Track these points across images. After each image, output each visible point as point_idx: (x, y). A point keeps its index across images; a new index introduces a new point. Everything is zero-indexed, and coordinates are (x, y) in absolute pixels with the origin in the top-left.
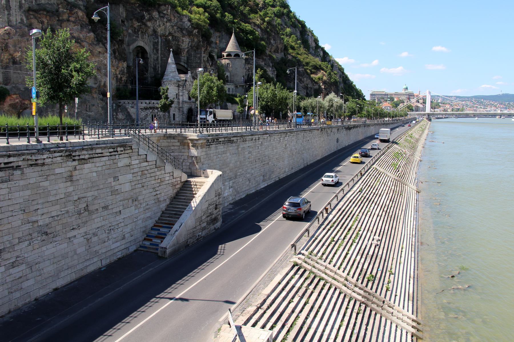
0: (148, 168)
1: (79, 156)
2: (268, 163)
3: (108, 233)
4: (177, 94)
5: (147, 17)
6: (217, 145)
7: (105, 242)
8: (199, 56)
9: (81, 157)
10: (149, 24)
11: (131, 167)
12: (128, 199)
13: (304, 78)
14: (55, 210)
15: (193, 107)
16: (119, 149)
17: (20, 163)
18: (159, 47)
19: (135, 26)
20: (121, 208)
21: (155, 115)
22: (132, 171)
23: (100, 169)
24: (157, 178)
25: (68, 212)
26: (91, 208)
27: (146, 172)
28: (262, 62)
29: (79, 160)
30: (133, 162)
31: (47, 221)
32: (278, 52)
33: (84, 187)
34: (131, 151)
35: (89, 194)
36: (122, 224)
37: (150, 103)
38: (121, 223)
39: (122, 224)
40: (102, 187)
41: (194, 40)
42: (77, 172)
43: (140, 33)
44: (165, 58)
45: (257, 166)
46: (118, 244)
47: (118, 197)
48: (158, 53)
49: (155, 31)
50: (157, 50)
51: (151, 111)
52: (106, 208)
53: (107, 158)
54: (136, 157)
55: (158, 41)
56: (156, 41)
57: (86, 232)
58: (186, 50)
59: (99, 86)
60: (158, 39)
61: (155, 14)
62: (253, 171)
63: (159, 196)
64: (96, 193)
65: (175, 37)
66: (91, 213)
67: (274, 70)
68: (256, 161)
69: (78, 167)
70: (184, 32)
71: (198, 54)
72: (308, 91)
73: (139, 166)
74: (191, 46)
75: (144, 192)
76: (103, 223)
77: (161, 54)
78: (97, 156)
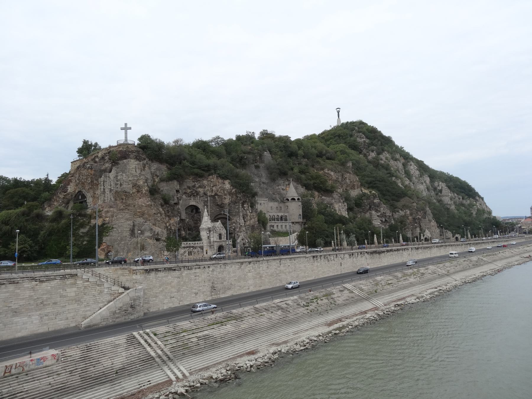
0: (89, 285)
1: (40, 279)
2: (222, 283)
3: (56, 316)
4: (208, 237)
6: (157, 272)
7: (53, 320)
8: (237, 207)
9: (41, 280)
11: (76, 285)
12: (73, 300)
13: (380, 208)
14: (22, 303)
15: (224, 245)
16: (66, 276)
17: (5, 283)
19: (188, 192)
20: (67, 304)
21: (191, 252)
22: (77, 287)
23: (53, 285)
24: (97, 290)
25: (29, 304)
26: (45, 303)
27: (88, 287)
29: (39, 281)
30: (78, 282)
31: (17, 307)
32: (355, 189)
33: (41, 293)
34: (77, 277)
35: (44, 296)
36: (67, 312)
37: (187, 244)
38: (66, 311)
39: (67, 312)
40: (54, 293)
41: (233, 197)
42: (38, 287)
43: (192, 196)
44: (213, 211)
45: (205, 284)
46: (63, 321)
47: (65, 298)
49: (205, 194)
51: (188, 249)
52: (55, 303)
53: (59, 280)
54: (80, 280)
55: (208, 200)
56: (206, 200)
57: (40, 314)
59: (154, 235)
60: (208, 198)
63: (98, 300)
64: (49, 296)
66: (44, 305)
67: (345, 205)
68: (204, 282)
69: (38, 284)
71: (237, 206)
72: (387, 219)
73: (82, 284)
75: (85, 297)
76: (53, 310)
78: (51, 279)
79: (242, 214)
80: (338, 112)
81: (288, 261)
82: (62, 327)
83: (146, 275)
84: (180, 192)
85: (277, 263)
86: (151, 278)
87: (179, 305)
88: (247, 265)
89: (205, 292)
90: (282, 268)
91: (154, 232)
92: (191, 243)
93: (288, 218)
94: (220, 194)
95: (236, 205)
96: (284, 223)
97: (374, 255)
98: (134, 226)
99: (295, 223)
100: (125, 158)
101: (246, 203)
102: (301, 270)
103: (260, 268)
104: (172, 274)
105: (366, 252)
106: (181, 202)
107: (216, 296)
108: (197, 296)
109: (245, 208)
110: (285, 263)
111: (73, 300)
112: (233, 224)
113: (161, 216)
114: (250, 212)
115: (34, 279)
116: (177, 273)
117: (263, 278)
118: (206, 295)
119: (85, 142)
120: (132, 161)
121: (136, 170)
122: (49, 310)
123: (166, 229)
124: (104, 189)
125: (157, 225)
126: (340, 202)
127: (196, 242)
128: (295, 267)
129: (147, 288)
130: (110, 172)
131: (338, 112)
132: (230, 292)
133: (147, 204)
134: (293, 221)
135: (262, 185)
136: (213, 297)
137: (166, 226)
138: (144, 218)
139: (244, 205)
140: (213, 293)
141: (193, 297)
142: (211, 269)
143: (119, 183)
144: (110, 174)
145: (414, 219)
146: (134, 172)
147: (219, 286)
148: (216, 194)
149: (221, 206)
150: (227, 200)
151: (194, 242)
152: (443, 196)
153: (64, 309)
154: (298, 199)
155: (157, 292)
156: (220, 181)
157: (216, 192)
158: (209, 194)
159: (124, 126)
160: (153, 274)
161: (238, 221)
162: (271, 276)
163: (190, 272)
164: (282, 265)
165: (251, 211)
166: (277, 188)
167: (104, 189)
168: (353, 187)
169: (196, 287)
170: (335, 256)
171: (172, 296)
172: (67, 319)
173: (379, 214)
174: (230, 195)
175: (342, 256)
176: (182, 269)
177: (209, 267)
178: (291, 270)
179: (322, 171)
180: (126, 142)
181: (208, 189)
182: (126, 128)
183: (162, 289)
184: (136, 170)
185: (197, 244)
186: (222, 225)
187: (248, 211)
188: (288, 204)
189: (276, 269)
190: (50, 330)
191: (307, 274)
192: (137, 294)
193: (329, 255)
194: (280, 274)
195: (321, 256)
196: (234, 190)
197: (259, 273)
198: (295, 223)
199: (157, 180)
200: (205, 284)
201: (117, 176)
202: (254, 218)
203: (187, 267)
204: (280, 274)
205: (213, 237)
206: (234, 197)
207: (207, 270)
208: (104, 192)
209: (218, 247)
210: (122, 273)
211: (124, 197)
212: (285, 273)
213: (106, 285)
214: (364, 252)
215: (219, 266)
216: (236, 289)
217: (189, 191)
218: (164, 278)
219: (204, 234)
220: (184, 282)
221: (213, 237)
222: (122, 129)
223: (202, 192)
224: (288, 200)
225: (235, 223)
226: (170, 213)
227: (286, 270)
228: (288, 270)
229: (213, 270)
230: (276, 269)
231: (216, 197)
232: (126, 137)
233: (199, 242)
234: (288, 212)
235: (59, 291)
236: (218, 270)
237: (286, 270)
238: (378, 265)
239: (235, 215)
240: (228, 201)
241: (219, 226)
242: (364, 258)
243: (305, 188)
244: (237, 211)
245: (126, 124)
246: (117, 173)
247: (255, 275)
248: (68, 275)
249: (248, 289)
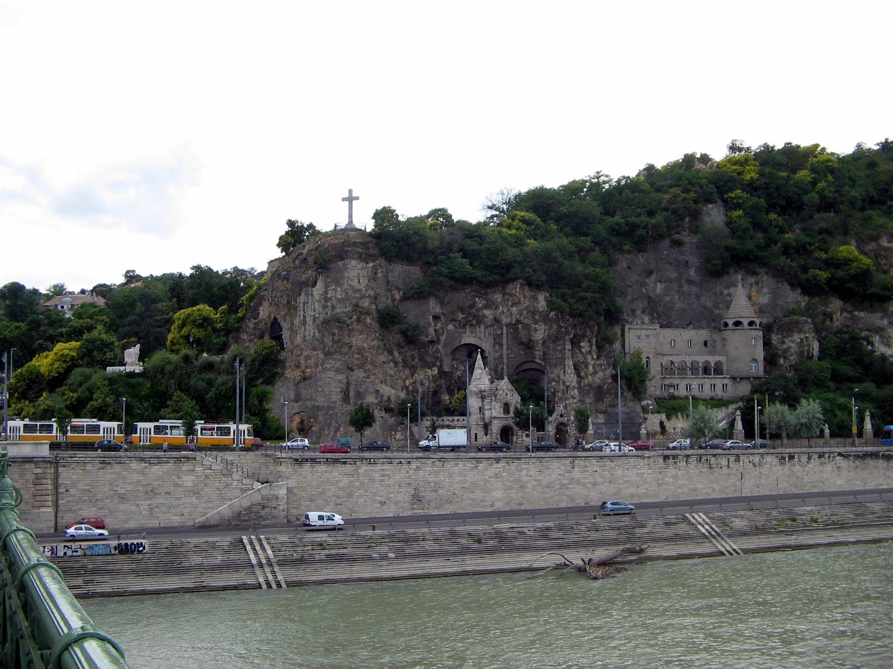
2: (436, 491)
4: (480, 408)
5: (480, 303)
8: (560, 348)
10: (487, 312)
14: (129, 488)
18: (504, 341)
19: (460, 319)
20: (182, 496)
28: (882, 318)
30: (197, 469)
31: (124, 492)
42: (147, 470)
43: (468, 326)
45: (401, 490)
46: (177, 517)
48: (502, 349)
49: (497, 321)
50: (501, 345)
52: (168, 493)
55: (502, 333)
56: (499, 332)
58: (541, 342)
59: (381, 402)
60: (502, 329)
62: (391, 495)
64: (160, 483)
65: (526, 325)
66: (155, 494)
68: (399, 486)
70: (537, 317)
71: (560, 345)
74: (548, 335)
75: (206, 490)
77: (508, 349)
79: (571, 363)
81: (594, 461)
82: (176, 524)
83: (296, 467)
84: (442, 318)
85: (565, 465)
86: (304, 472)
87: (350, 518)
88: (491, 465)
89: (399, 502)
90: (577, 473)
91: (382, 396)
92: (445, 418)
93: (725, 368)
94: (526, 321)
95: (557, 343)
96: (706, 380)
97: (871, 462)
98: (348, 384)
99: (738, 380)
100: (342, 258)
101: (586, 339)
102: (626, 481)
103: (521, 471)
104: (340, 469)
105: (840, 454)
106: (443, 338)
107: (421, 511)
108: (384, 507)
109: (583, 350)
110: (586, 466)
111: (190, 492)
112: (551, 383)
113: (396, 366)
114: (593, 359)
115: (142, 459)
116: (348, 468)
117: (527, 490)
118: (402, 507)
119: (291, 223)
120: (354, 262)
121: (359, 280)
122: (160, 500)
123: (405, 391)
124: (304, 317)
125: (388, 383)
127: (456, 418)
128: (612, 475)
129: (296, 485)
130: (314, 284)
132: (451, 507)
133: (372, 344)
134: (736, 375)
135: (686, 288)
136: (415, 511)
137: (405, 386)
138: (365, 371)
139: (582, 344)
140: (415, 506)
141: (377, 508)
142: (413, 466)
143: (329, 304)
144: (313, 289)
146: (355, 283)
147: (428, 495)
148: (518, 322)
149: (529, 346)
150: (540, 333)
151: (450, 418)
153: (178, 501)
154: (751, 323)
155: (313, 493)
156: (528, 293)
157: (518, 316)
158: (505, 320)
159: (347, 195)
160: (307, 467)
161: (562, 376)
162: (548, 487)
163: (374, 468)
164: (576, 469)
165: (595, 357)
166: (726, 292)
167: (304, 317)
169: (382, 494)
170: (732, 459)
171: (340, 503)
172: (182, 515)
174: (545, 322)
175: (757, 459)
176: (358, 463)
177: (409, 463)
178: (599, 480)
179: (874, 244)
180: (349, 227)
181: (503, 311)
182: (350, 199)
183: (321, 490)
184: (359, 280)
186: (510, 387)
187: (589, 357)
188: (727, 334)
189: (560, 475)
190: (162, 525)
191: (645, 491)
192: (272, 492)
193: (715, 455)
194: (570, 486)
195: (688, 456)
196: (553, 314)
197: (519, 481)
198: (738, 380)
199: (397, 297)
200: (401, 490)
201: (326, 292)
202: (603, 371)
203: (366, 459)
204: (570, 486)
205: (490, 409)
206: (555, 327)
207: (405, 466)
208: (304, 322)
209: (499, 430)
210: (264, 461)
211: (336, 331)
212: (584, 485)
213: (235, 477)
214: (832, 453)
215: (429, 462)
216: (464, 504)
217: (461, 316)
218: (327, 474)
219: (473, 403)
220: (361, 483)
221: (490, 409)
222: (344, 199)
223: (491, 317)
224: (726, 325)
225: (556, 381)
226: (416, 360)
227: (586, 478)
228: (591, 479)
229: (418, 468)
230: (560, 475)
231: (520, 326)
232: (350, 216)
233: (461, 418)
234: (727, 355)
235: (173, 477)
236: (428, 469)
237: (586, 478)
238: (882, 485)
239: (556, 365)
240: (542, 336)
241: (505, 388)
242: (829, 467)
243: (799, 291)
244: (560, 356)
245: (350, 191)
246: (326, 287)
247: (509, 484)
248: (184, 458)
249: (491, 506)
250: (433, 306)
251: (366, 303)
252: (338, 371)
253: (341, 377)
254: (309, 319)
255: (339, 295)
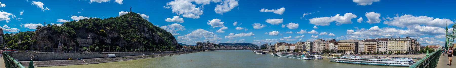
10: (61, 36)
49: (62, 37)
61: (62, 35)
80: (131, 8)
106: (55, 39)
126: (108, 39)
131: (131, 8)
145: (135, 45)
149: (65, 40)
150: (67, 39)
152: (155, 38)
154: (91, 38)
168: (115, 35)
173: (122, 43)
185: (57, 49)
217: (58, 37)
250: (54, 36)
251: (47, 35)
252: (43, 43)
253: (44, 44)
254: (40, 37)
255: (44, 34)
